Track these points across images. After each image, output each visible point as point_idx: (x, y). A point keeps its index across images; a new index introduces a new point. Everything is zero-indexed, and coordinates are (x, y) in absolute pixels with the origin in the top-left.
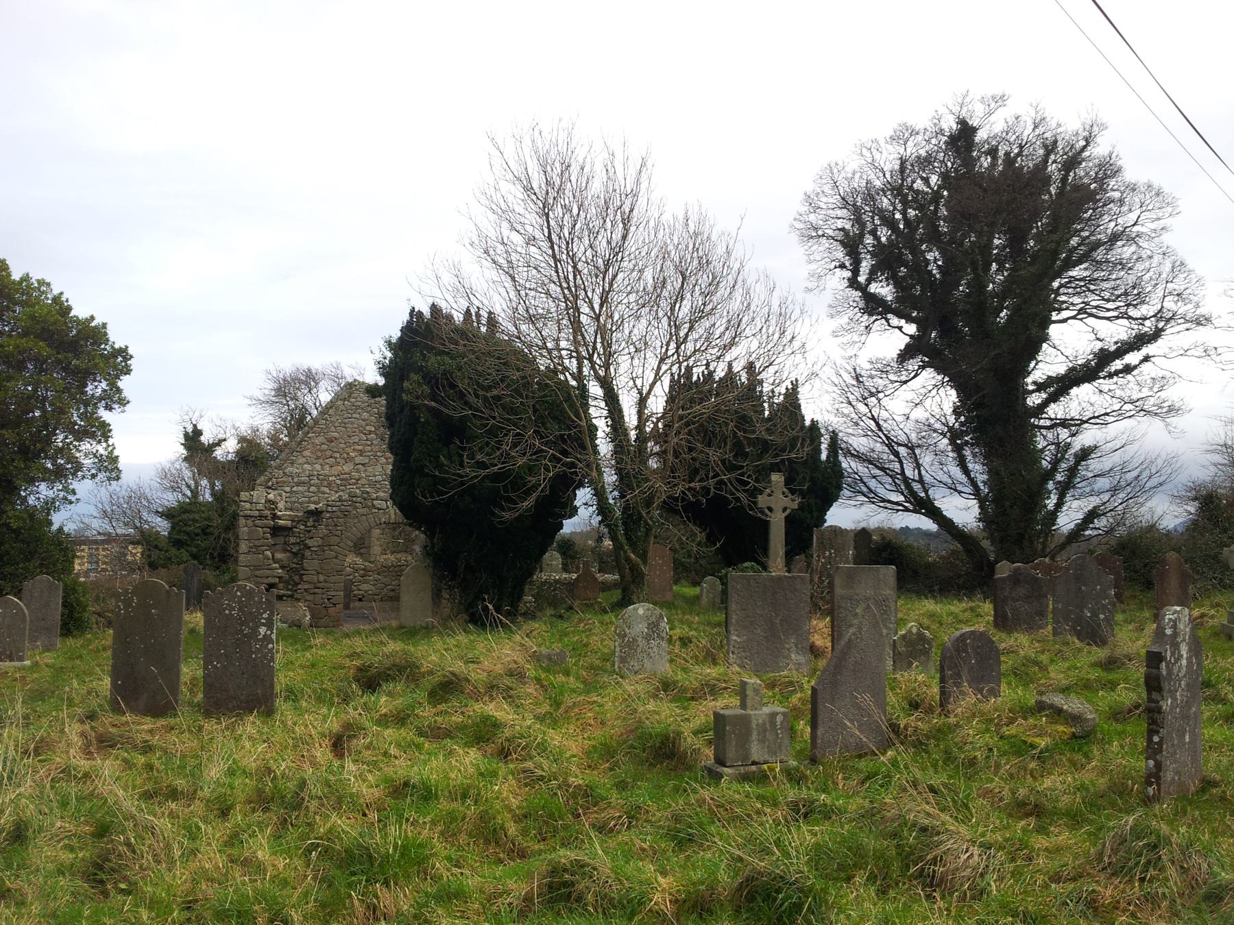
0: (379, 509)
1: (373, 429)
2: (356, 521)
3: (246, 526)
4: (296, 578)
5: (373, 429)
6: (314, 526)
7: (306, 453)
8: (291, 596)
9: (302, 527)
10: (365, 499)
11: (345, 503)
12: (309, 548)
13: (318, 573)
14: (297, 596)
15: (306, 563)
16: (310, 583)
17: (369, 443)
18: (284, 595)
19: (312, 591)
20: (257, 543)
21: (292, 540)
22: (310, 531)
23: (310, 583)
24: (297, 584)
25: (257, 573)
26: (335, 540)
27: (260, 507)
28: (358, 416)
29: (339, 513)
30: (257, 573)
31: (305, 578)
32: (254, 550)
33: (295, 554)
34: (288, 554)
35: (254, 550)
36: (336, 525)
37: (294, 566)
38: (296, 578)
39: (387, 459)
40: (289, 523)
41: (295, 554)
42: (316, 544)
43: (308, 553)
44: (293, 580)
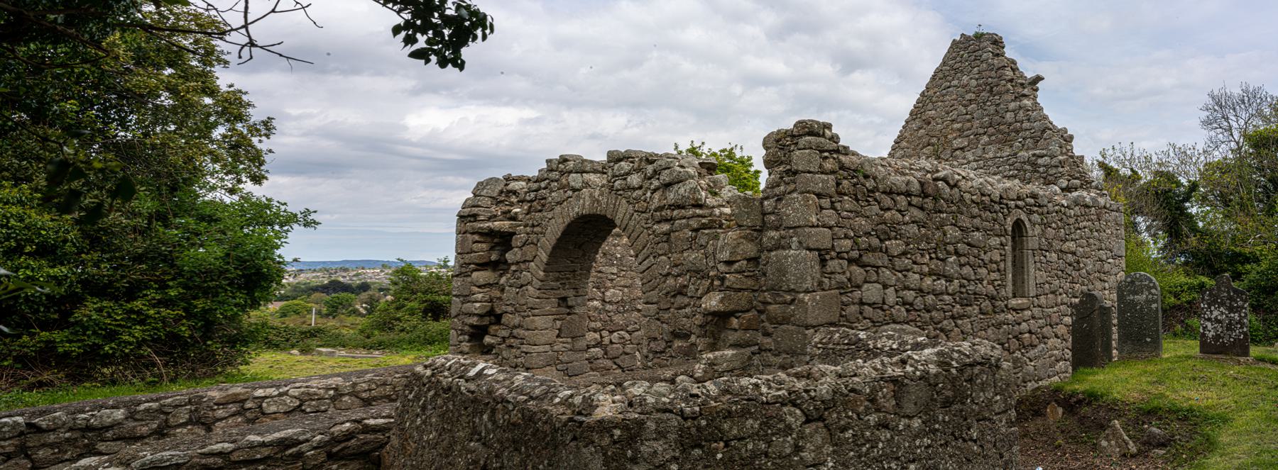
0: (574, 190)
10: (562, 173)
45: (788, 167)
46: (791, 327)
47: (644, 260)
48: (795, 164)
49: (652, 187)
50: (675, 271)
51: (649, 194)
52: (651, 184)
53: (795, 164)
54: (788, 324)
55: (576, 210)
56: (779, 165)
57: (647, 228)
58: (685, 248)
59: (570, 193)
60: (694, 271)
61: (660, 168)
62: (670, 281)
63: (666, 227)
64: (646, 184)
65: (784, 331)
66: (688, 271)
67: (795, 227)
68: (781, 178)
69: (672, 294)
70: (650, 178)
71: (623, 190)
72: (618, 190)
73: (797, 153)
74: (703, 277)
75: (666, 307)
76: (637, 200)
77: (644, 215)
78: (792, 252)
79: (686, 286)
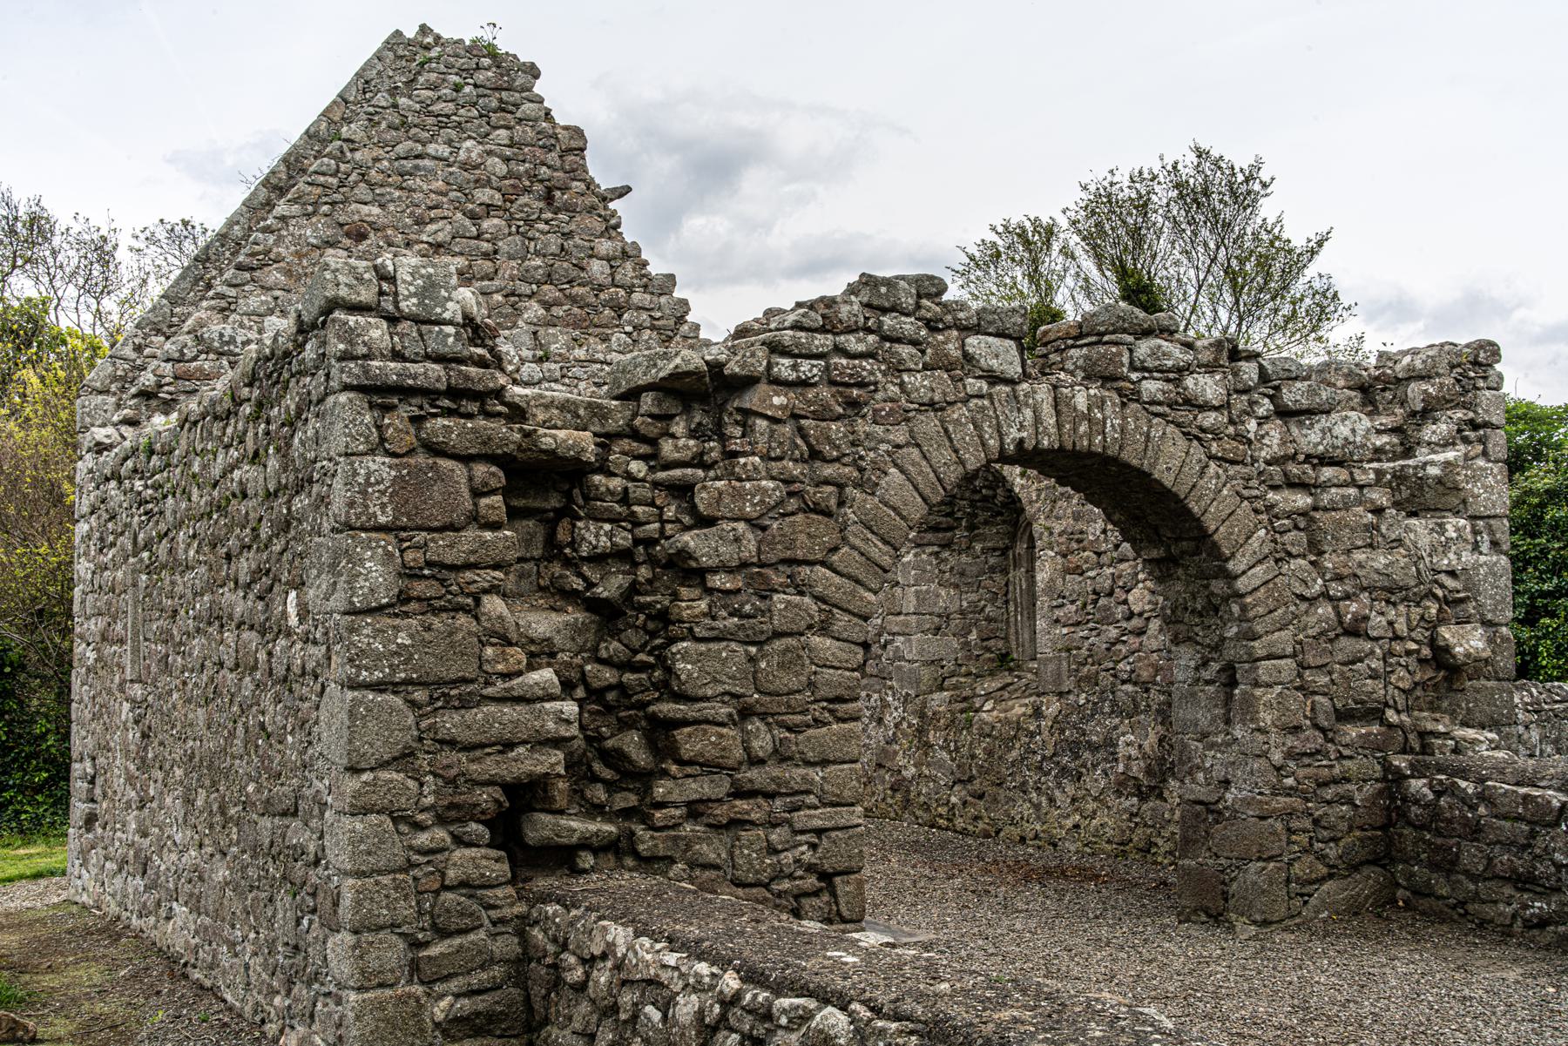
0: (994, 378)
1: (497, 198)
2: (899, 435)
3: (380, 446)
4: (632, 744)
5: (497, 198)
6: (698, 461)
7: (274, 276)
8: (617, 849)
9: (637, 467)
10: (932, 326)
11: (853, 343)
12: (696, 575)
13: (746, 713)
14: (646, 841)
15: (687, 661)
16: (711, 767)
17: (486, 246)
18: (585, 845)
19: (721, 813)
20: (442, 547)
21: (596, 536)
22: (683, 491)
23: (711, 767)
24: (645, 779)
25: (450, 723)
26: (807, 534)
27: (449, 338)
28: (444, 151)
29: (826, 393)
30: (450, 723)
31: (691, 743)
32: (419, 588)
33: (607, 614)
34: (574, 615)
35: (419, 588)
36: (815, 455)
37: (609, 676)
38: (632, 744)
39: (547, 306)
40: (585, 442)
41: (607, 614)
42: (727, 552)
43: (692, 604)
44: (615, 758)
45: (1471, 415)
46: (1483, 682)
47: (1253, 566)
48: (1487, 411)
49: (1261, 411)
50: (1336, 589)
51: (1252, 425)
52: (1252, 403)
53: (1487, 411)
54: (1478, 679)
55: (1014, 433)
56: (1451, 408)
57: (1247, 498)
58: (1360, 543)
59: (974, 385)
60: (1383, 589)
61: (1282, 374)
62: (1324, 610)
63: (1302, 500)
64: (1240, 402)
65: (1477, 691)
66: (1364, 589)
67: (1489, 517)
68: (1459, 431)
69: (1332, 635)
70: (1246, 391)
71: (1170, 406)
72: (1153, 403)
73: (1487, 393)
74: (1402, 600)
75: (1320, 662)
76: (1217, 435)
77: (1238, 468)
78: (1483, 559)
79: (1366, 618)
